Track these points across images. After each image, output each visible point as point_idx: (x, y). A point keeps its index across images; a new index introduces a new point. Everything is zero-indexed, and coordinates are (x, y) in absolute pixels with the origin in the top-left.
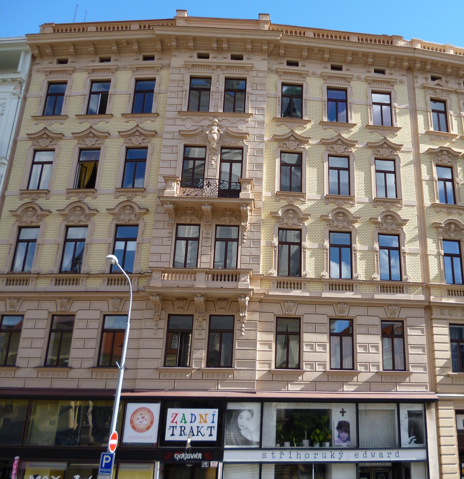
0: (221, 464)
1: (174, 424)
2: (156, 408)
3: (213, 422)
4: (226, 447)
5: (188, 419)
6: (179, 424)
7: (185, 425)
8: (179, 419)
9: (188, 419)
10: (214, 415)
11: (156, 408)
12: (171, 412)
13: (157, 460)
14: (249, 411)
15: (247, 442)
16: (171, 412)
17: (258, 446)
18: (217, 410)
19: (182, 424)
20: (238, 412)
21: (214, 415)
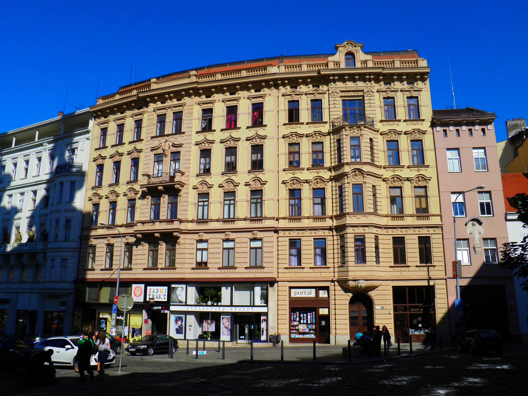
0: (169, 312)
1: (150, 294)
2: (142, 286)
3: (165, 293)
4: (171, 304)
5: (155, 291)
6: (152, 294)
7: (154, 294)
8: (152, 291)
9: (155, 291)
10: (166, 289)
11: (142, 286)
12: (148, 288)
13: (144, 309)
14: (181, 287)
15: (181, 302)
16: (148, 288)
17: (185, 304)
18: (167, 287)
19: (153, 294)
20: (177, 288)
21: (166, 289)
